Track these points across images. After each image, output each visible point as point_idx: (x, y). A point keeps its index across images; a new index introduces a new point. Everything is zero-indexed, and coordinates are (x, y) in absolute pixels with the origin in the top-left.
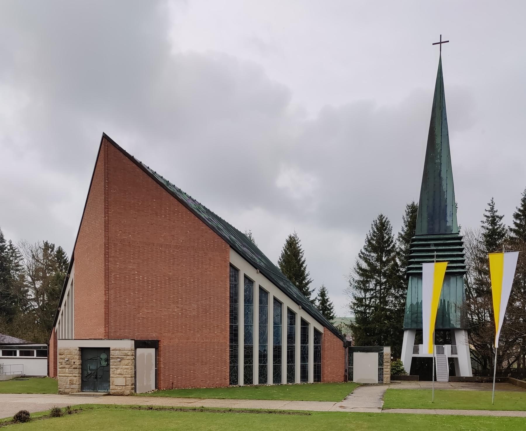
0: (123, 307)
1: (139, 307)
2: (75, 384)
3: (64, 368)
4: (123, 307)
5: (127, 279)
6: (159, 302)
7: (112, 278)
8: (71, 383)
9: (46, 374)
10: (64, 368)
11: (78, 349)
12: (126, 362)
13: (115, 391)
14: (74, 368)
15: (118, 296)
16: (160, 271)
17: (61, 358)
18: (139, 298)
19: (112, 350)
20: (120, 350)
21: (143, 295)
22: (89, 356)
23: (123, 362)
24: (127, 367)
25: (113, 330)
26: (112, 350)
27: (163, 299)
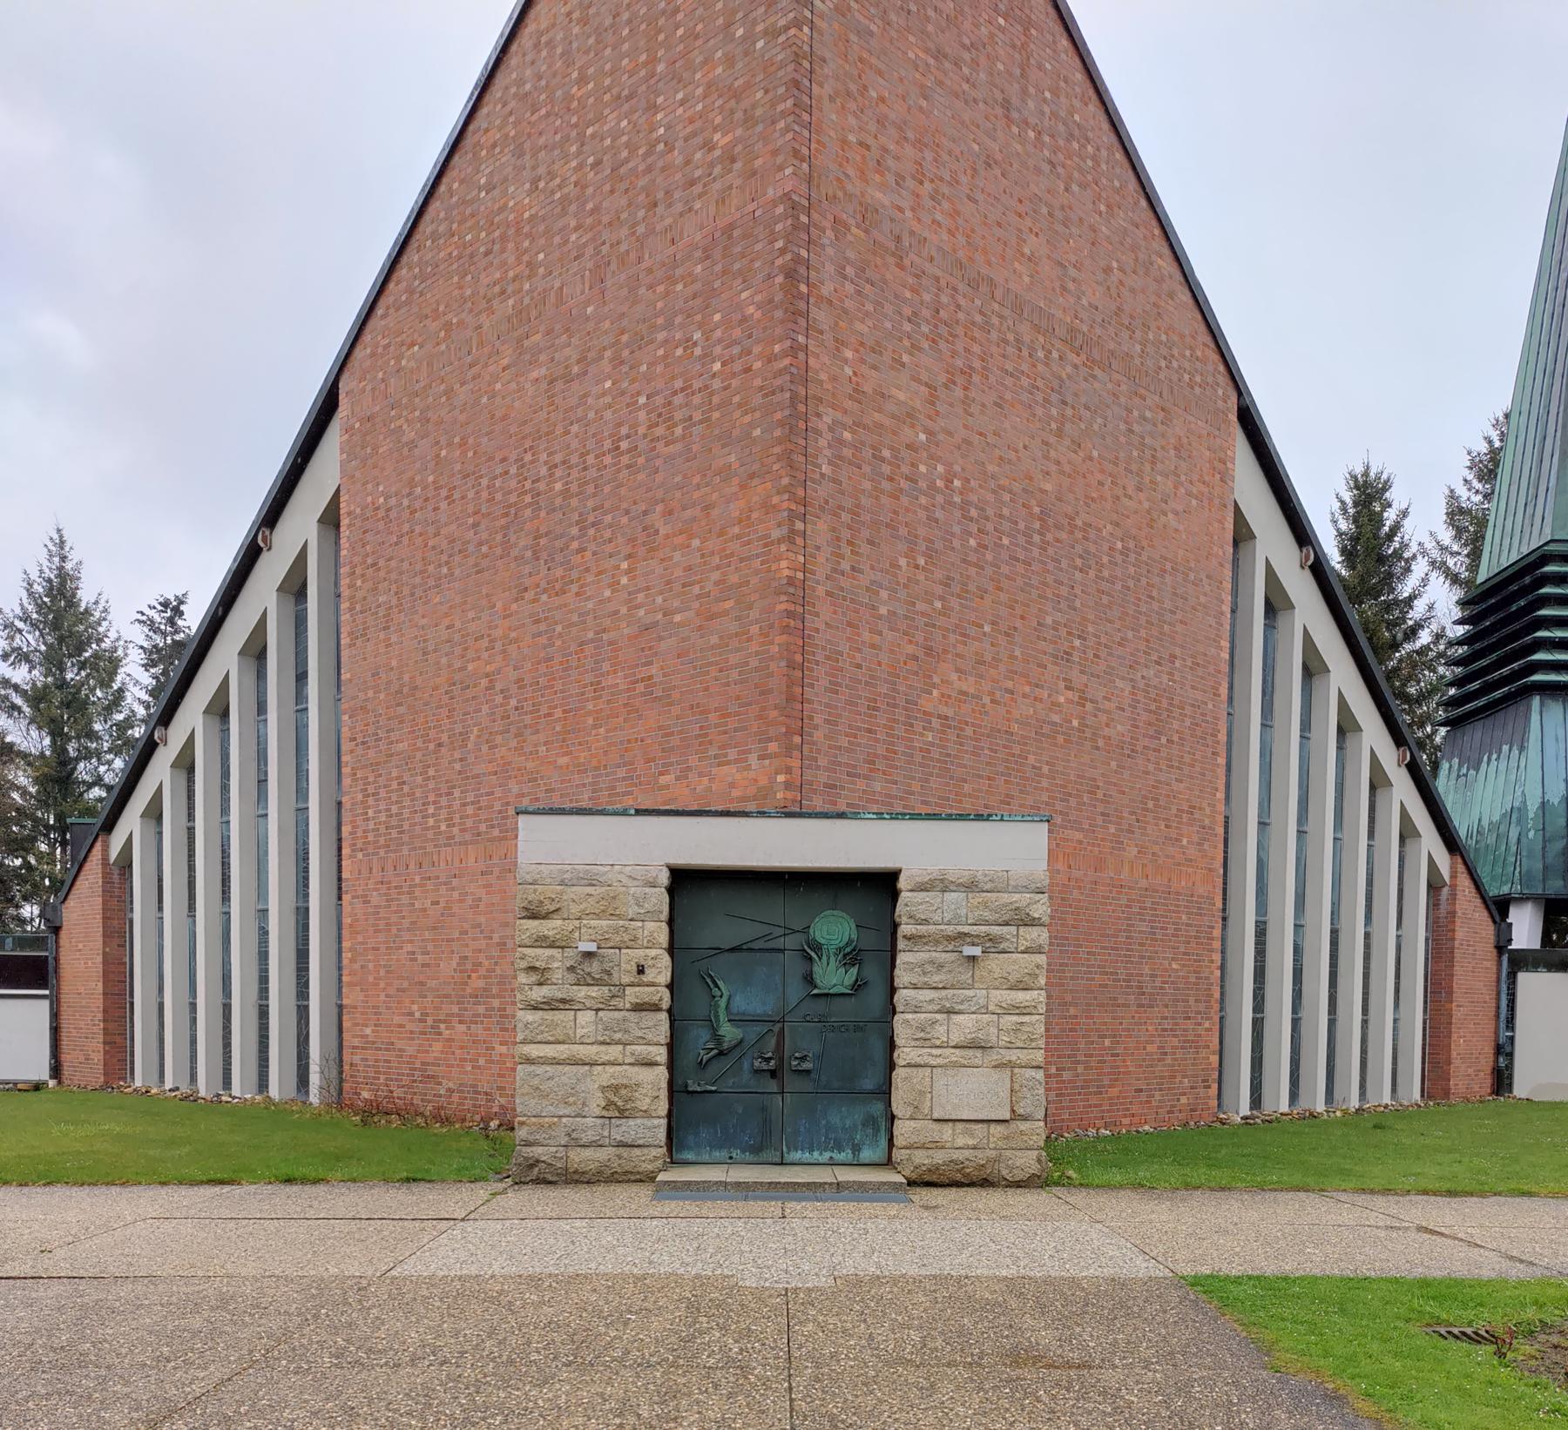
0: (866, 636)
1: (929, 651)
2: (647, 1114)
3: (564, 1004)
6: (1002, 640)
7: (822, 442)
8: (618, 1107)
9: (41, 1072)
10: (564, 1004)
11: (664, 878)
13: (939, 1157)
14: (638, 1008)
16: (1012, 455)
17: (542, 941)
19: (921, 888)
20: (971, 886)
21: (946, 583)
22: (722, 925)
23: (996, 965)
24: (1021, 997)
25: (823, 777)
26: (921, 888)
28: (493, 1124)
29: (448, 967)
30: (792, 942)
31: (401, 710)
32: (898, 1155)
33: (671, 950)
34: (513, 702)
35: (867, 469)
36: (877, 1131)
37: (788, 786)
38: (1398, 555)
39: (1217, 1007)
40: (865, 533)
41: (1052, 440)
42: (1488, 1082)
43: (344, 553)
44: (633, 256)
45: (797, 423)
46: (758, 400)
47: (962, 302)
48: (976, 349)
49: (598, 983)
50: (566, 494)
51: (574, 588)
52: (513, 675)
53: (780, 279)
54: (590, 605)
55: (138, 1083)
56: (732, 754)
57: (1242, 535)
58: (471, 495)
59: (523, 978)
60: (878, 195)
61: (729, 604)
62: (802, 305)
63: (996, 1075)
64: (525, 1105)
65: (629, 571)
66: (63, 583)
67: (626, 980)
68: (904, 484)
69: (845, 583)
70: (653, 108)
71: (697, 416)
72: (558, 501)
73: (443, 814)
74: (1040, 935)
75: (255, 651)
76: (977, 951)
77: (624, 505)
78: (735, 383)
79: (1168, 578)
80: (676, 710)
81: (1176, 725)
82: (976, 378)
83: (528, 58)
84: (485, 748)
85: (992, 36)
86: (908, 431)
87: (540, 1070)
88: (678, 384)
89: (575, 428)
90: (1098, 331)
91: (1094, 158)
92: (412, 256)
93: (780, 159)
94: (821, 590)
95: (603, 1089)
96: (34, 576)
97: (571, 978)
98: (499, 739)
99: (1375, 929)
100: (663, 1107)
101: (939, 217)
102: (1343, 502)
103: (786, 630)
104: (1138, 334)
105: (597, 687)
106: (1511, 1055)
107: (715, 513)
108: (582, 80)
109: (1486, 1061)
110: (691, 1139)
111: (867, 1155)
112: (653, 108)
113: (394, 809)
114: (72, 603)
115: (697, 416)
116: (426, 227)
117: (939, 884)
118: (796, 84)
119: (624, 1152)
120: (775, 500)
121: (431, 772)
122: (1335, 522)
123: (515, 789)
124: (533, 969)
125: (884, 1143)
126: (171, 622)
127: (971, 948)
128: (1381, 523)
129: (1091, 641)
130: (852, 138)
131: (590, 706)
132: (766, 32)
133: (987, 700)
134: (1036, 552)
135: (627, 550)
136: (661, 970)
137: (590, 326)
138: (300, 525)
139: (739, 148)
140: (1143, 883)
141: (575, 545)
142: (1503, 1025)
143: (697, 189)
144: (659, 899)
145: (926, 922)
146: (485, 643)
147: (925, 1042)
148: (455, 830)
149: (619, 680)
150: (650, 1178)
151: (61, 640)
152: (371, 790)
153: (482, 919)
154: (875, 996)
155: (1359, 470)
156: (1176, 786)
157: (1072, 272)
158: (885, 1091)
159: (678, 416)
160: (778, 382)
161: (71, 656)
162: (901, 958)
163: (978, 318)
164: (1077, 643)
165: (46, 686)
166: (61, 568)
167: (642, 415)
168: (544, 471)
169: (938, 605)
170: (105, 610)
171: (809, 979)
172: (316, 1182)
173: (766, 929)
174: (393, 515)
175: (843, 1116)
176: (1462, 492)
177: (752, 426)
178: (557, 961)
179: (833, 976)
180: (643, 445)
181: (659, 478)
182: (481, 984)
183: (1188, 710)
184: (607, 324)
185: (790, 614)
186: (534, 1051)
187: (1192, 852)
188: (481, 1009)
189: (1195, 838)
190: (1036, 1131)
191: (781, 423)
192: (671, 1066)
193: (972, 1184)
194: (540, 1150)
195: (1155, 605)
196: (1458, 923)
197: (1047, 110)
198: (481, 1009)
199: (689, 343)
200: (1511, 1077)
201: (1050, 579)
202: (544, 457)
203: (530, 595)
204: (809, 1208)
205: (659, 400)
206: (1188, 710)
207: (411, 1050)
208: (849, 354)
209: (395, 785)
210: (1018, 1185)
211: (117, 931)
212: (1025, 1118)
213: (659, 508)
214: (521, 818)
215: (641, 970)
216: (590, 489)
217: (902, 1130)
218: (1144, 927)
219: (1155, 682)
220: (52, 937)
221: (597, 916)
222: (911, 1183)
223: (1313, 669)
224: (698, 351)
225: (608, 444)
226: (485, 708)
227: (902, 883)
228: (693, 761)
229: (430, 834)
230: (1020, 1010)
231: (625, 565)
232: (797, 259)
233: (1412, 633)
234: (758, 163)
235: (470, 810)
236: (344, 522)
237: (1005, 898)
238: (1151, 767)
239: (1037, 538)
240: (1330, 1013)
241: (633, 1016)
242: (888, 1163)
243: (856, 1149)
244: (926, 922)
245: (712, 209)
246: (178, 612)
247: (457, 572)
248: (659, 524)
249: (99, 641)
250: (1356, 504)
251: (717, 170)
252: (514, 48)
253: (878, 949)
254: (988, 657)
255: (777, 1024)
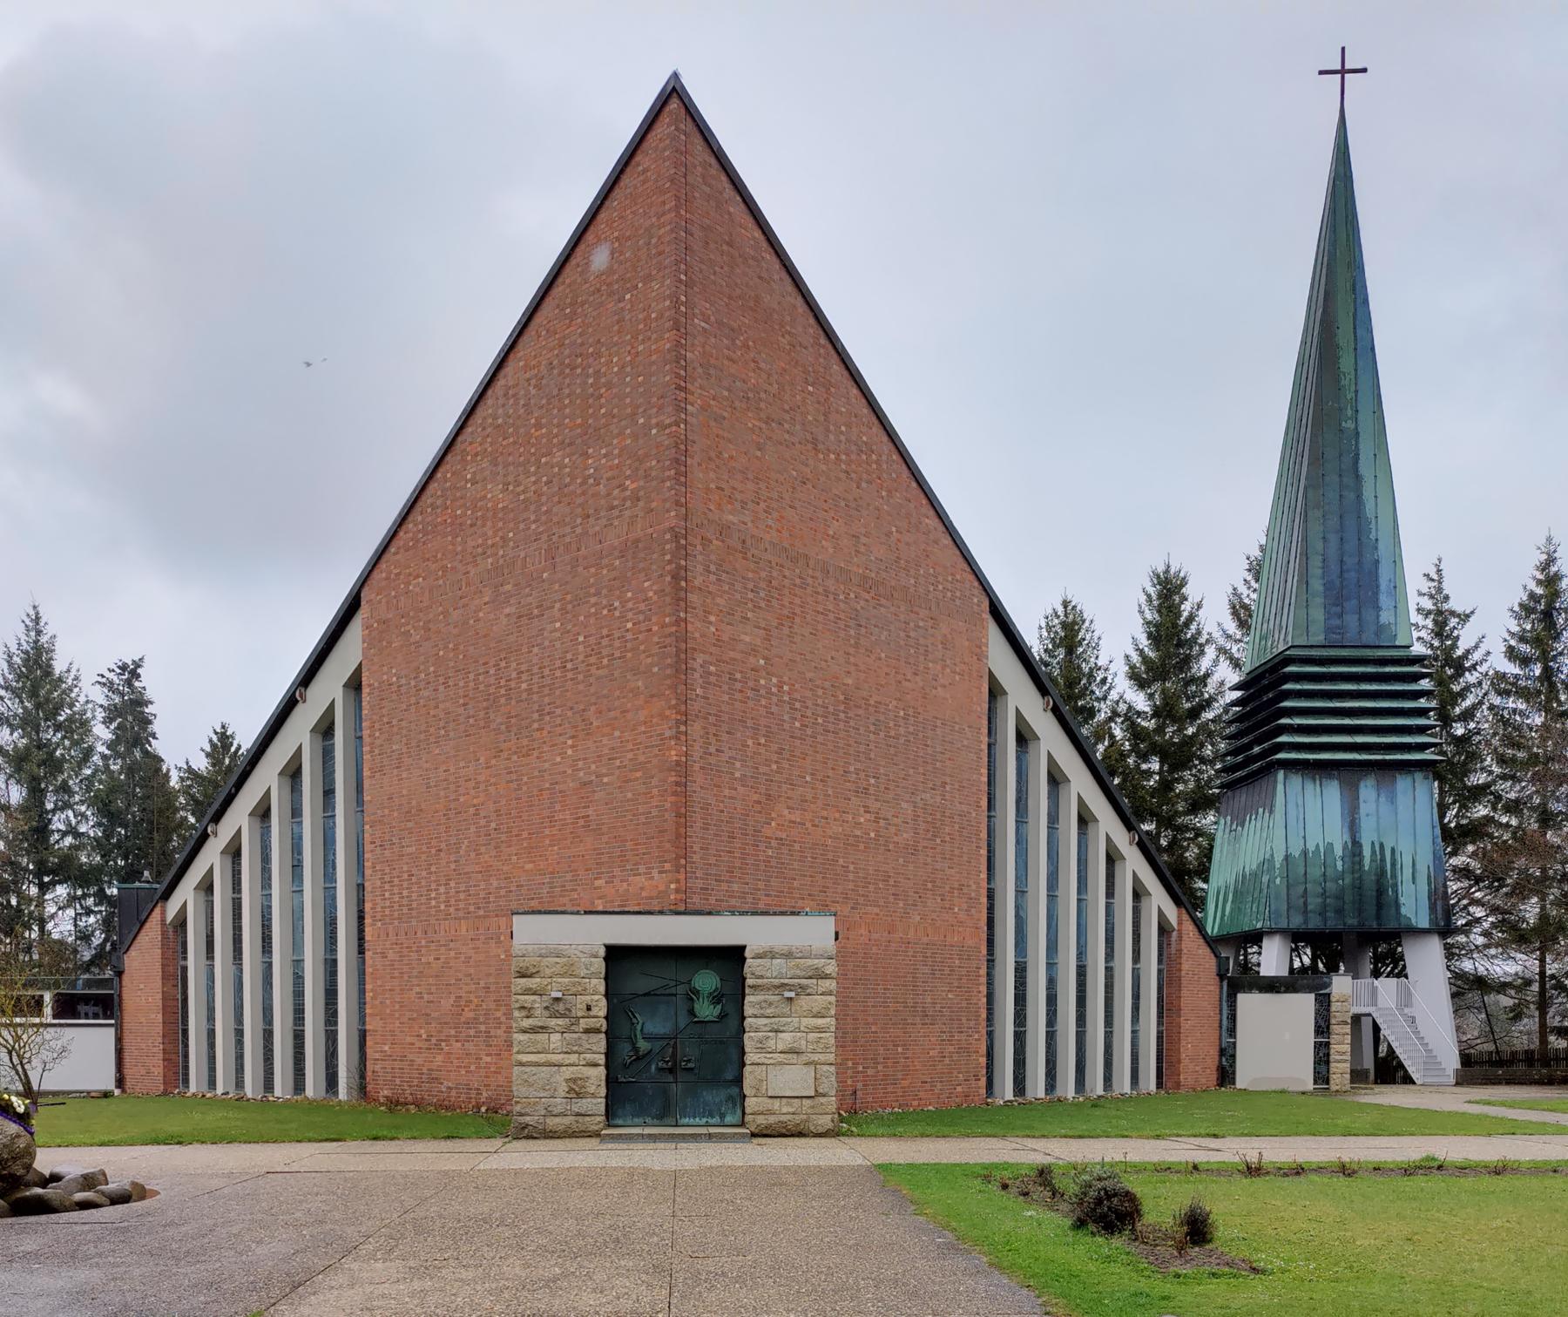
0: (726, 792)
2: (593, 1096)
3: (543, 1029)
4: (726, 792)
5: (738, 686)
6: (819, 785)
7: (697, 675)
8: (576, 1091)
9: (109, 1084)
10: (543, 1029)
11: (602, 952)
12: (819, 1002)
13: (772, 1119)
14: (587, 1031)
15: (712, 749)
18: (767, 762)
20: (788, 955)
21: (780, 752)
22: (639, 981)
23: (804, 1002)
24: (820, 1021)
25: (700, 883)
27: (830, 773)
28: (483, 1109)
29: (447, 1003)
30: (681, 989)
31: (410, 825)
32: (748, 1118)
33: (607, 995)
34: (493, 825)
35: (725, 687)
36: (735, 1105)
37: (677, 891)
38: (1194, 639)
39: (984, 1024)
40: (725, 727)
41: (852, 651)
42: (1213, 1077)
43: (365, 712)
44: (574, 546)
45: (682, 667)
46: (655, 650)
47: (787, 573)
48: (797, 601)
49: (563, 1016)
50: (529, 691)
51: (536, 753)
52: (492, 807)
53: (668, 578)
54: (547, 765)
55: (193, 1088)
56: (642, 869)
57: (995, 692)
58: (461, 684)
59: (516, 1014)
60: (731, 517)
61: (639, 774)
62: (682, 594)
63: (805, 1069)
64: (519, 1090)
65: (572, 747)
66: (39, 655)
67: (580, 1014)
68: (750, 693)
69: (712, 760)
70: (586, 455)
71: (617, 654)
72: (524, 695)
73: (443, 898)
74: (831, 985)
75: (293, 773)
76: (792, 994)
77: (569, 704)
78: (641, 637)
79: (939, 731)
80: (605, 838)
81: (947, 830)
82: (797, 620)
83: (501, 402)
84: (473, 855)
85: (804, 400)
86: (752, 660)
87: (528, 1069)
88: (605, 632)
89: (536, 650)
90: (884, 574)
91: (877, 462)
92: (416, 516)
93: (668, 505)
94: (696, 767)
95: (567, 1081)
96: (14, 649)
97: (547, 1013)
98: (483, 849)
99: (1116, 964)
100: (603, 1091)
101: (770, 522)
102: (1149, 596)
103: (675, 794)
104: (912, 572)
105: (551, 819)
106: (1233, 1056)
107: (629, 716)
108: (538, 426)
109: (1212, 1060)
110: (620, 1112)
111: (728, 1119)
112: (586, 455)
113: (405, 893)
114: (48, 671)
115: (617, 654)
116: (427, 499)
117: (770, 954)
118: (677, 461)
119: (580, 1119)
120: (668, 713)
121: (433, 869)
122: (1141, 612)
123: (495, 884)
124: (523, 1008)
125: (739, 1112)
126: (129, 683)
127: (789, 993)
128: (1179, 614)
129: (883, 779)
130: (713, 486)
131: (547, 832)
132: (657, 425)
133: (808, 825)
134: (842, 725)
135: (571, 732)
136: (601, 1009)
137: (546, 586)
138: (329, 688)
139: (642, 493)
140: (925, 940)
141: (536, 725)
142: (1224, 1034)
143: (616, 512)
144: (599, 965)
145: (762, 977)
146: (472, 784)
147: (761, 1050)
148: (452, 910)
149: (567, 816)
150: (597, 1135)
151: (38, 706)
152: (387, 878)
153: (472, 971)
154: (732, 1022)
155: (1161, 569)
156: (948, 872)
157: (863, 540)
158: (739, 1081)
159: (605, 652)
160: (668, 641)
161: (46, 720)
162: (748, 999)
163: (798, 581)
164: (872, 781)
165: (27, 748)
166: (36, 642)
167: (581, 648)
168: (514, 675)
169: (774, 767)
170: (76, 678)
171: (692, 1013)
172: (392, 1139)
173: (665, 982)
174: (403, 689)
175: (711, 1096)
176: (1243, 590)
177: (652, 665)
178: (537, 1002)
179: (706, 1011)
180: (582, 667)
181: (592, 690)
182: (472, 1015)
183: (957, 819)
184: (557, 587)
185: (677, 784)
186: (524, 1058)
187: (962, 916)
188: (472, 1032)
189: (965, 906)
190: (831, 1103)
191: (670, 666)
192: (607, 1067)
193: (792, 1136)
194: (528, 1118)
195: (930, 750)
196: (1184, 958)
197: (843, 438)
198: (472, 1032)
199: (611, 609)
200: (1234, 1073)
201: (852, 742)
202: (514, 665)
203: (505, 755)
204: (692, 1145)
205: (592, 640)
206: (957, 819)
207: (419, 1061)
208: (712, 618)
209: (405, 876)
210: (820, 1135)
211: (176, 978)
212: (824, 1095)
213: (593, 708)
214: (515, 918)
215: (589, 1008)
216: (546, 691)
217: (751, 1103)
218: (926, 970)
219: (931, 801)
220: (116, 979)
221: (562, 976)
222: (753, 1135)
223: (1056, 779)
224: (617, 614)
225: (558, 663)
226: (473, 828)
227: (747, 954)
228: (617, 872)
229: (433, 911)
230: (820, 1030)
231: (570, 742)
232: (679, 567)
233: (1208, 704)
234: (654, 505)
235: (462, 896)
236: (365, 690)
237: (809, 962)
238: (929, 860)
239: (842, 715)
240: (1078, 1025)
241: (584, 1036)
242: (742, 1124)
243: (722, 1116)
244: (762, 977)
245: (625, 528)
246: (135, 675)
247: (452, 734)
248: (593, 719)
249: (71, 706)
250: (1160, 596)
251: (628, 504)
252: (490, 392)
253: (733, 992)
254: (809, 797)
255: (671, 1040)
